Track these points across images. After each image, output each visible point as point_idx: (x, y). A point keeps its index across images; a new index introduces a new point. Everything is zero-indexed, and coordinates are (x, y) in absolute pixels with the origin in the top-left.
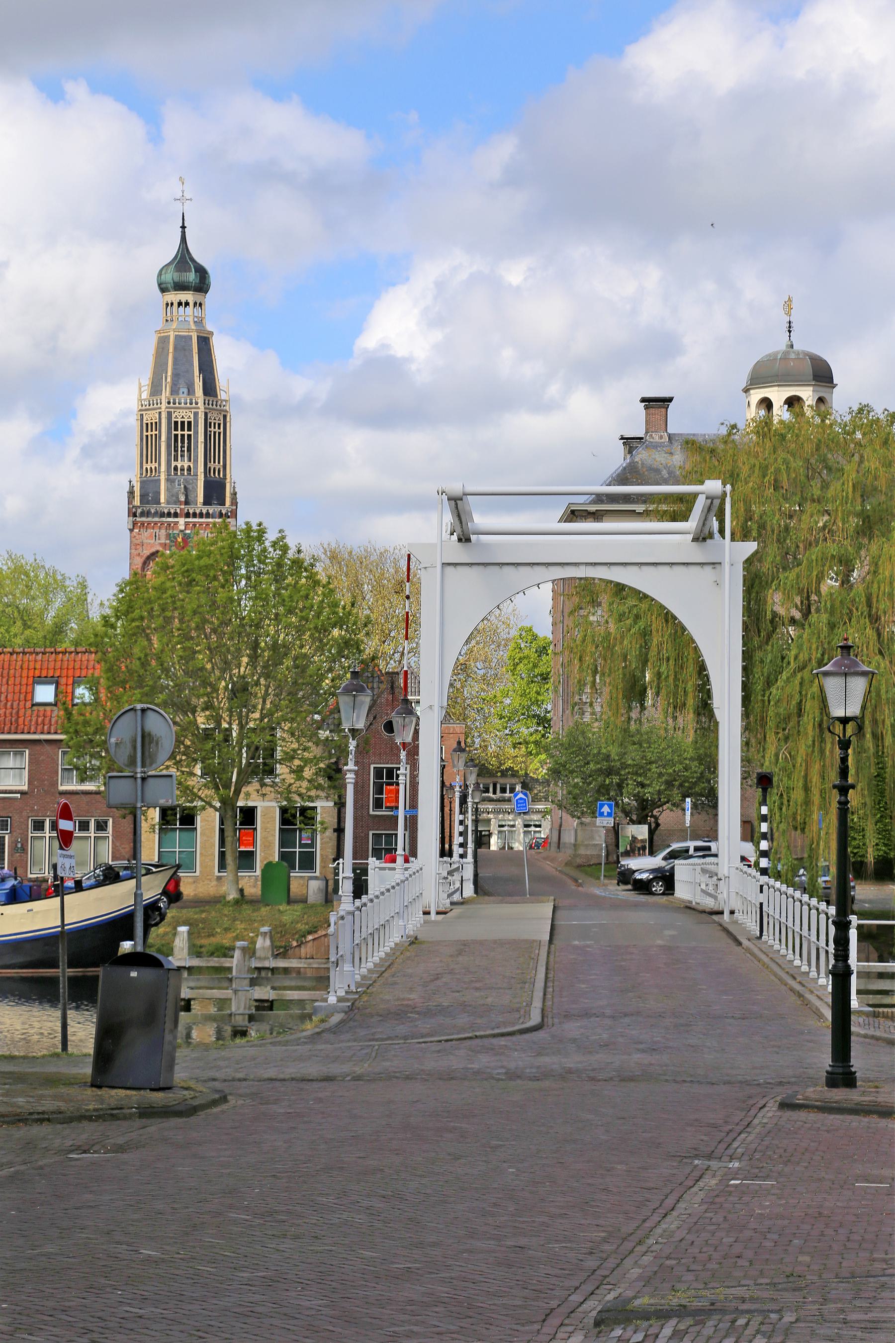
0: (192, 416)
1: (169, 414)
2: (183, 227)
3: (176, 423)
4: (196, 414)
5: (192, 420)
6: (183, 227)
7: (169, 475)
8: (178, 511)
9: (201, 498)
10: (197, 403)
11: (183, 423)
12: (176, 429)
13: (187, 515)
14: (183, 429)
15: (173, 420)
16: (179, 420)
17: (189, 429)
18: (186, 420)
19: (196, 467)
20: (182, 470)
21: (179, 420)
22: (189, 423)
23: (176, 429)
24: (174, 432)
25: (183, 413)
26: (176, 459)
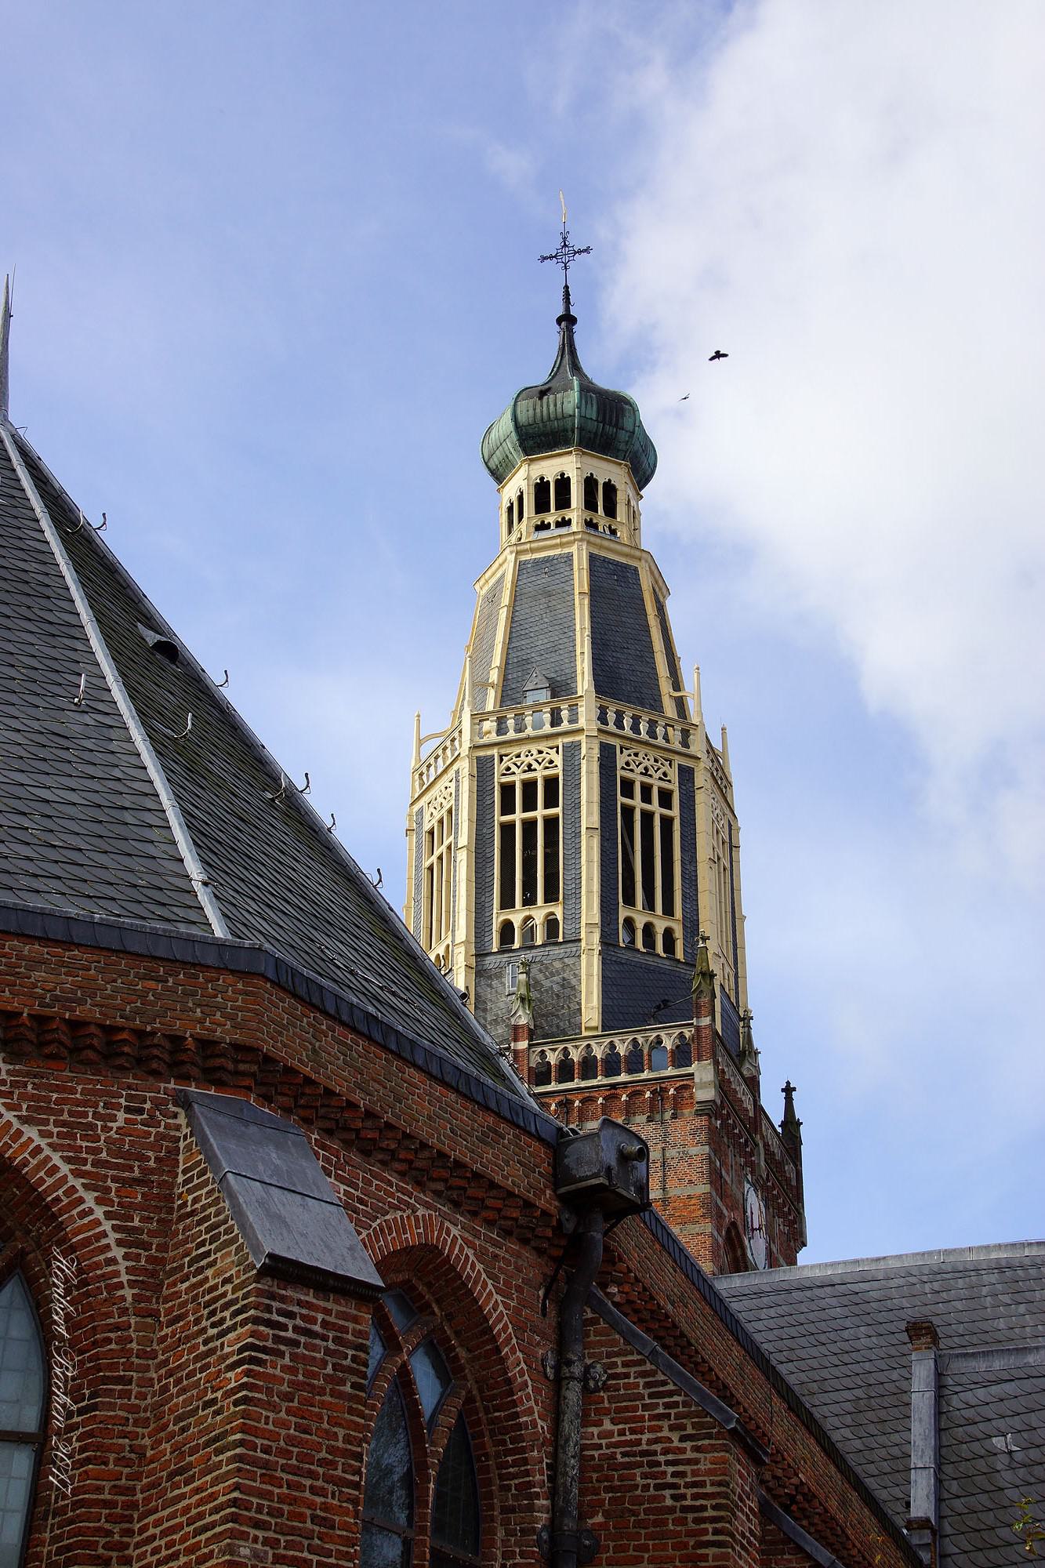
0: (558, 760)
2: (567, 320)
3: (508, 790)
4: (571, 753)
5: (559, 771)
6: (567, 320)
7: (481, 954)
9: (591, 1012)
10: (573, 720)
11: (529, 787)
12: (508, 808)
14: (529, 805)
15: (498, 779)
16: (518, 778)
17: (551, 801)
18: (539, 775)
19: (573, 916)
20: (529, 933)
21: (518, 778)
22: (551, 783)
23: (508, 808)
24: (499, 818)
25: (529, 754)
26: (507, 902)
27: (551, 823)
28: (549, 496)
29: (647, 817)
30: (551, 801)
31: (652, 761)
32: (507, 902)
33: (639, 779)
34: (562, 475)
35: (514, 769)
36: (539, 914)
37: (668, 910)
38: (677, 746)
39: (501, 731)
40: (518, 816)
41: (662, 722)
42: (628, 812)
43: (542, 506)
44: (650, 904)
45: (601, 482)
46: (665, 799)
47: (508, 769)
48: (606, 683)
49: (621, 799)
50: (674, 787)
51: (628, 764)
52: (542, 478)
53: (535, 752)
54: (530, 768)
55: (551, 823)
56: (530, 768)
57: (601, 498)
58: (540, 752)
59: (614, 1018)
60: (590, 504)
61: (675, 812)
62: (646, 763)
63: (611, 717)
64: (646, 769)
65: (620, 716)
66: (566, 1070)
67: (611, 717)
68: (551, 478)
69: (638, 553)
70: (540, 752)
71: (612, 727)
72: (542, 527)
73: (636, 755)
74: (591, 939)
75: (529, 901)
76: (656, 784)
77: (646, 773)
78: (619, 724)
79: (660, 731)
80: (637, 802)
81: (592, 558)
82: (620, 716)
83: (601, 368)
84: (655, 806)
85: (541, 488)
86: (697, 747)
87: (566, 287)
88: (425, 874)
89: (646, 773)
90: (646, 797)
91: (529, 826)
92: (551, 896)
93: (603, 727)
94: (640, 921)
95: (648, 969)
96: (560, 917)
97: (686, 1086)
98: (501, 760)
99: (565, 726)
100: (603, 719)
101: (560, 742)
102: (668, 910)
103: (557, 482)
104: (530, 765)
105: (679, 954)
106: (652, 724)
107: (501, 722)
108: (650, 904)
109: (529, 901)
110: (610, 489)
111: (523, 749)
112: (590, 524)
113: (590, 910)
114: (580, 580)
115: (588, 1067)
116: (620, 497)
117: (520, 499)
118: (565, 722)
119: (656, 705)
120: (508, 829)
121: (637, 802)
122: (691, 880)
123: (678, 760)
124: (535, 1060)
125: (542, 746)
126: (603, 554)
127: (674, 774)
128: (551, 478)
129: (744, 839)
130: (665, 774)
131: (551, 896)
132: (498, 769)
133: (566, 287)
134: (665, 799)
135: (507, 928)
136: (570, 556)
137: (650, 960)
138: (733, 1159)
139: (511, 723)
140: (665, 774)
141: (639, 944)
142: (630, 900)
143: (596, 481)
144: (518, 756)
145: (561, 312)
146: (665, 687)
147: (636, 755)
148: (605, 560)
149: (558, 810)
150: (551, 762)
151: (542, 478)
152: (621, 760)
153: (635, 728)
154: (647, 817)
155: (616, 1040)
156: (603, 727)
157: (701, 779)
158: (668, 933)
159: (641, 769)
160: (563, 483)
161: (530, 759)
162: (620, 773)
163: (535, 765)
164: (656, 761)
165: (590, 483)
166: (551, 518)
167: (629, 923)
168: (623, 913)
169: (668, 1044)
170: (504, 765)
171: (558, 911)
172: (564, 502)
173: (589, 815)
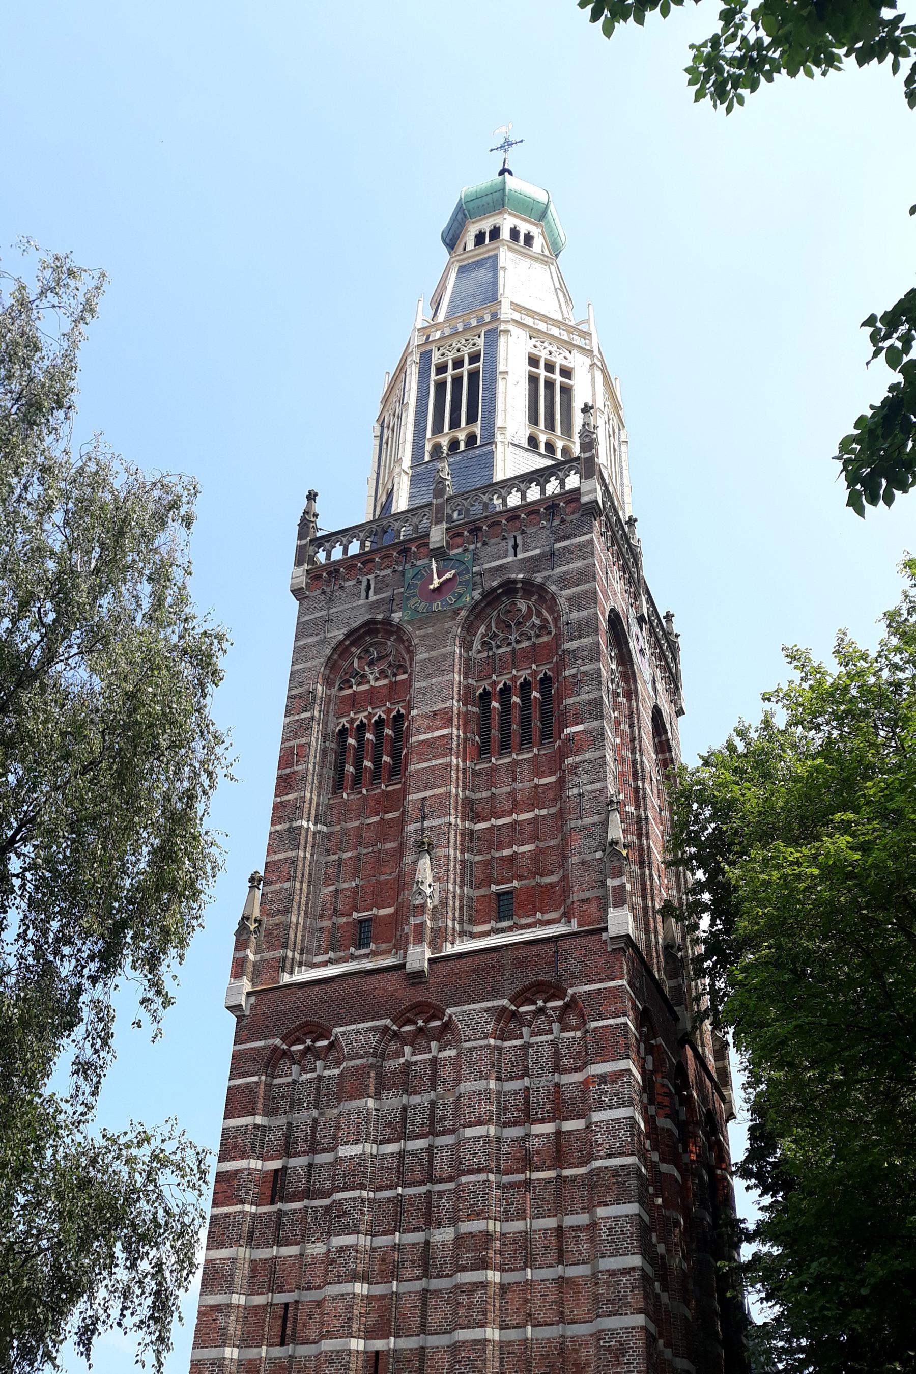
0: (481, 342)
1: (426, 356)
32: (438, 428)
33: (543, 355)
36: (462, 436)
44: (550, 426)
47: (443, 355)
53: (463, 342)
94: (543, 438)
108: (550, 426)
131: (472, 419)
135: (437, 448)
161: (459, 345)
171: (477, 429)
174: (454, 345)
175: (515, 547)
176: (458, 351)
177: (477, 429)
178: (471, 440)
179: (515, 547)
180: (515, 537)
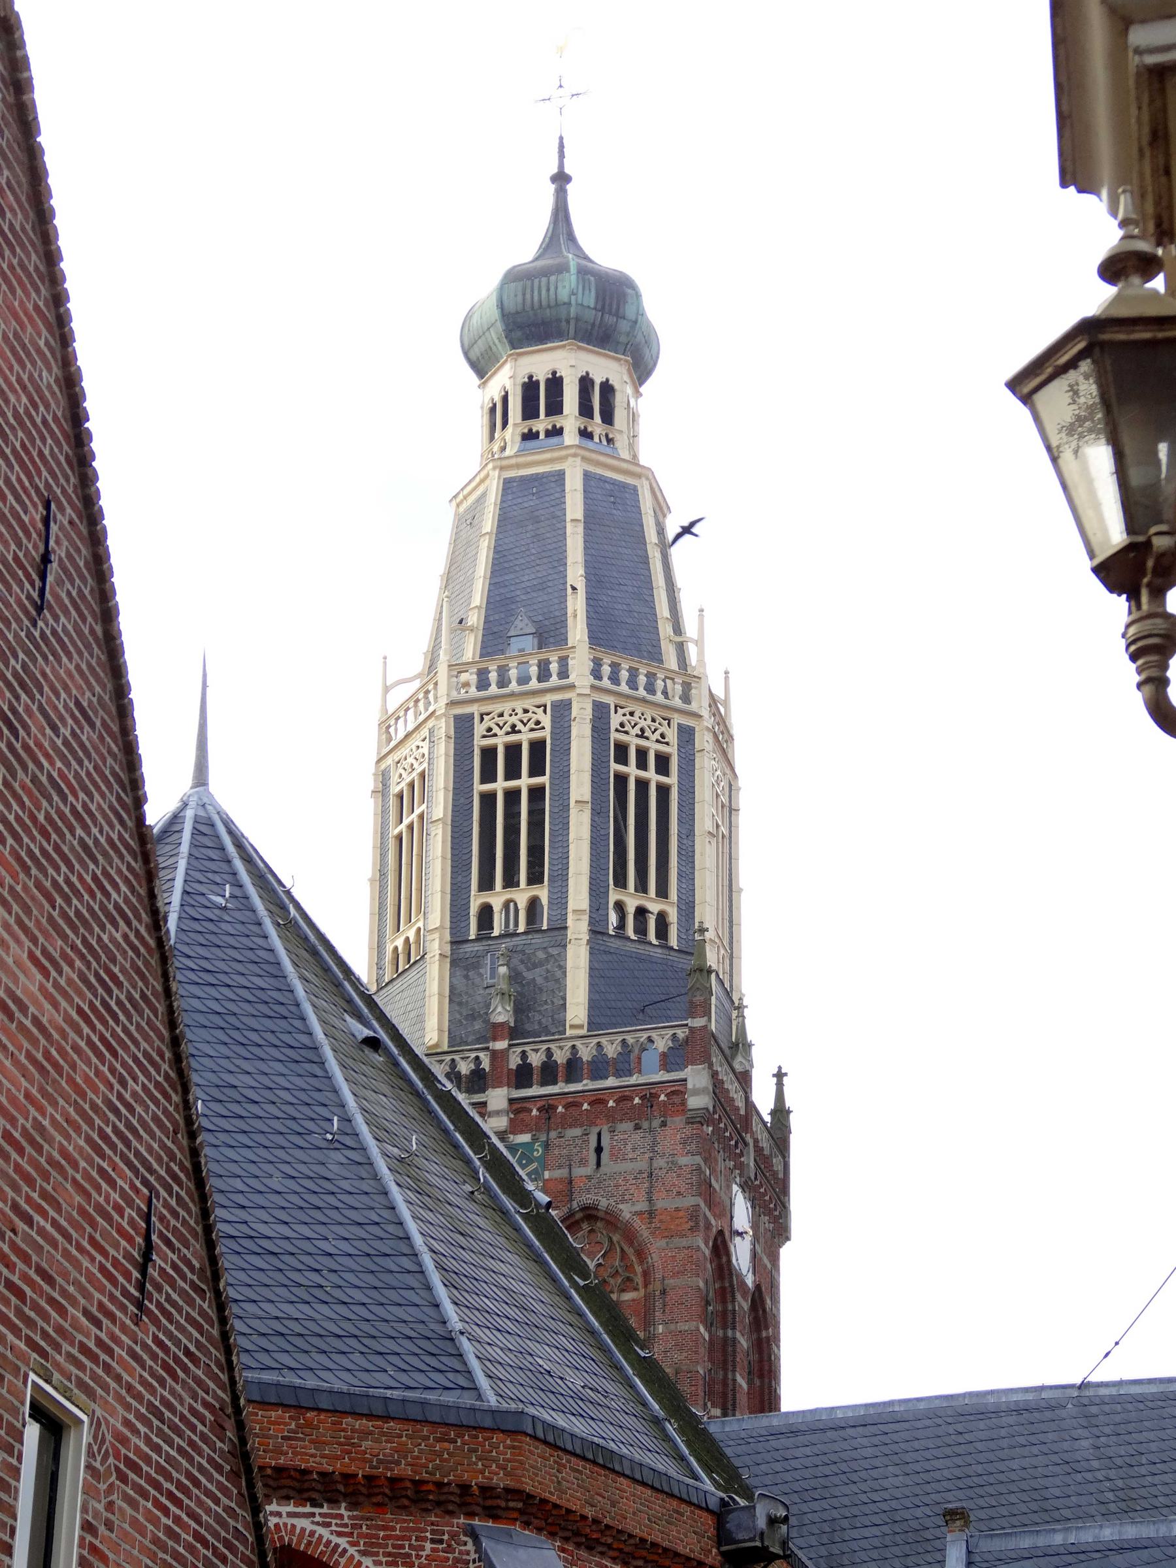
0: (546, 721)
2: (561, 179)
3: (489, 754)
4: (562, 712)
5: (546, 734)
6: (561, 179)
7: (458, 941)
8: (486, 1064)
9: (577, 1009)
10: (564, 673)
11: (513, 751)
12: (488, 775)
13: (523, 1075)
14: (513, 772)
15: (479, 742)
16: (500, 742)
17: (537, 768)
18: (525, 738)
19: (560, 899)
21: (500, 742)
22: (537, 748)
23: (488, 775)
24: (479, 788)
26: (486, 884)
27: (537, 793)
28: (540, 397)
29: (642, 785)
30: (537, 768)
31: (649, 722)
32: (486, 884)
33: (633, 742)
34: (554, 373)
35: (496, 730)
36: (522, 897)
37: (662, 892)
38: (677, 702)
39: (483, 684)
40: (500, 785)
41: (661, 675)
42: (621, 780)
43: (529, 412)
44: (642, 887)
45: (598, 381)
46: (663, 764)
47: (489, 730)
48: (602, 634)
49: (615, 767)
50: (673, 750)
51: (622, 725)
52: (530, 377)
53: (520, 711)
54: (514, 730)
55: (537, 793)
56: (514, 730)
57: (600, 402)
58: (526, 711)
59: (602, 1015)
60: (585, 410)
61: (672, 780)
62: (642, 723)
63: (606, 670)
64: (642, 730)
65: (615, 667)
66: (549, 1073)
67: (606, 670)
68: (541, 376)
69: (637, 470)
70: (526, 711)
71: (606, 683)
72: (530, 436)
73: (632, 714)
74: (578, 929)
75: (511, 881)
76: (653, 747)
77: (642, 735)
78: (615, 679)
79: (660, 684)
80: (632, 770)
81: (587, 476)
82: (615, 667)
83: (603, 245)
84: (651, 775)
85: (530, 388)
86: (699, 704)
87: (561, 138)
88: (392, 845)
89: (642, 735)
90: (642, 764)
91: (512, 796)
92: (535, 878)
93: (597, 683)
94: (631, 905)
95: (640, 959)
96: (545, 901)
97: (678, 1091)
98: (482, 720)
99: (554, 680)
100: (596, 674)
101: (548, 699)
102: (662, 892)
103: (548, 380)
104: (513, 726)
105: (673, 942)
106: (651, 676)
107: (483, 675)
108: (642, 887)
109: (511, 881)
110: (607, 389)
111: (506, 707)
112: (585, 434)
113: (579, 896)
114: (574, 507)
115: (573, 1069)
116: (619, 401)
117: (505, 399)
118: (554, 677)
119: (655, 656)
120: (488, 800)
121: (632, 770)
122: (688, 856)
123: (677, 719)
124: (514, 1061)
125: (528, 703)
126: (599, 471)
127: (672, 735)
128: (541, 376)
129: (745, 801)
130: (663, 736)
131: (535, 878)
132: (479, 729)
133: (561, 138)
134: (663, 764)
136: (561, 475)
137: (641, 949)
138: (723, 1164)
139: (493, 676)
140: (663, 736)
141: (630, 932)
142: (621, 882)
143: (592, 382)
144: (501, 715)
145: (554, 170)
146: (665, 629)
147: (632, 714)
148: (603, 480)
149: (545, 780)
150: (538, 723)
151: (530, 377)
152: (615, 720)
153: (632, 683)
154: (642, 785)
155: (604, 1041)
156: (597, 683)
157: (703, 740)
158: (662, 918)
159: (637, 730)
160: (555, 383)
161: (514, 720)
162: (614, 736)
163: (520, 726)
164: (653, 720)
165: (585, 383)
166: (541, 424)
167: (620, 907)
168: (614, 896)
169: (662, 1044)
170: (485, 725)
172: (555, 408)
173: (580, 787)
174: (506, 717)
175: (599, 1150)
176: (513, 726)
177: (543, 893)
178: (534, 904)
179: (599, 1150)
180: (599, 1134)
